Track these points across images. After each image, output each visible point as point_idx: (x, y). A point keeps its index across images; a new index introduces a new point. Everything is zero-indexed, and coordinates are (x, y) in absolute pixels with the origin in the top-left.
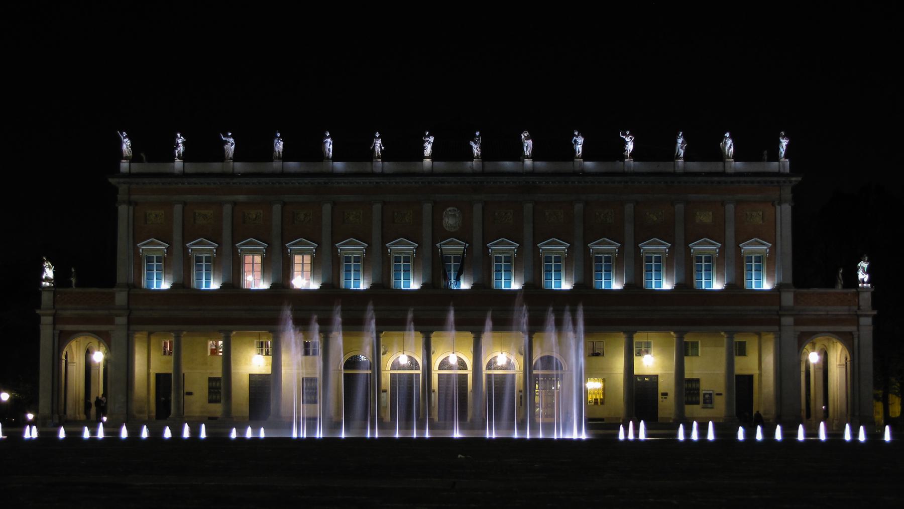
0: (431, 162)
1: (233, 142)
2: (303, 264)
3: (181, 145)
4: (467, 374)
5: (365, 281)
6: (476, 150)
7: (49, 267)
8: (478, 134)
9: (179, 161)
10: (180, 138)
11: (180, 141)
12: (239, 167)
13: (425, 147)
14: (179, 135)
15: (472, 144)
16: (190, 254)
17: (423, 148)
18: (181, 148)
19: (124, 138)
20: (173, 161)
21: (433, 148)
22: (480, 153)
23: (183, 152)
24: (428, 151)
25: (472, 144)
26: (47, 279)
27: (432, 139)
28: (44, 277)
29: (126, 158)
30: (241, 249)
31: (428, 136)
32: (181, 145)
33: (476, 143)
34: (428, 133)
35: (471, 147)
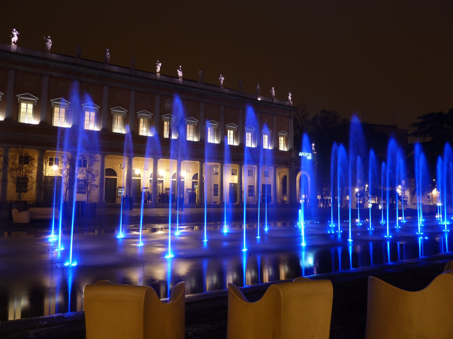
0: (160, 76)
1: (51, 42)
2: (90, 116)
3: (16, 36)
4: (140, 179)
5: (125, 130)
8: (180, 67)
9: (14, 45)
10: (15, 32)
11: (15, 33)
13: (157, 68)
14: (15, 30)
15: (178, 71)
16: (52, 106)
17: (157, 68)
22: (182, 76)
23: (17, 41)
24: (158, 69)
25: (178, 71)
27: (160, 64)
30: (53, 103)
31: (159, 63)
33: (180, 71)
34: (158, 61)
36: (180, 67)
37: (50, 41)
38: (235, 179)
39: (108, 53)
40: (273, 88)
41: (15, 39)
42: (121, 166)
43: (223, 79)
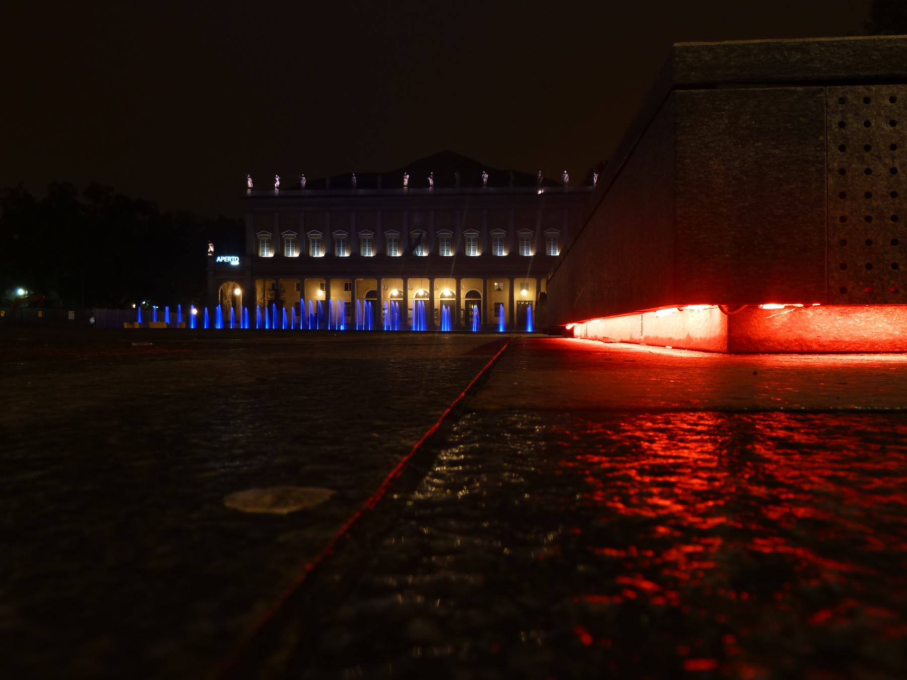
3: (278, 181)
6: (431, 182)
7: (212, 246)
11: (277, 179)
12: (308, 192)
14: (277, 176)
15: (429, 179)
17: (403, 181)
18: (278, 183)
19: (249, 178)
20: (274, 189)
21: (408, 181)
24: (406, 182)
25: (429, 179)
26: (211, 252)
27: (408, 176)
28: (209, 251)
29: (250, 188)
31: (406, 174)
32: (278, 181)
35: (429, 180)
36: (432, 173)
37: (304, 178)
38: (320, 294)
39: (354, 177)
40: (566, 172)
41: (278, 183)
42: (384, 287)
43: (486, 176)
